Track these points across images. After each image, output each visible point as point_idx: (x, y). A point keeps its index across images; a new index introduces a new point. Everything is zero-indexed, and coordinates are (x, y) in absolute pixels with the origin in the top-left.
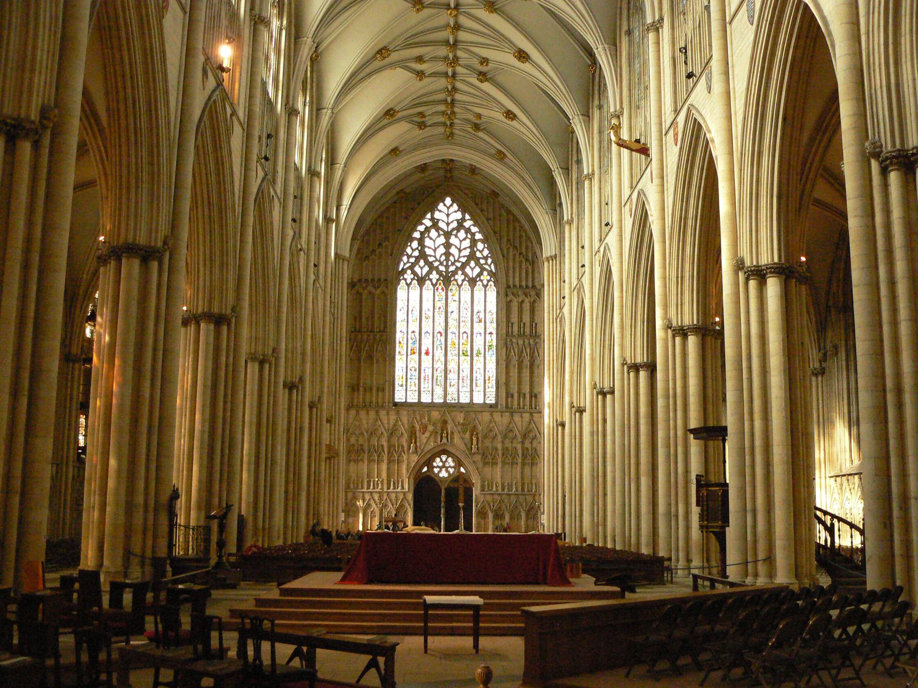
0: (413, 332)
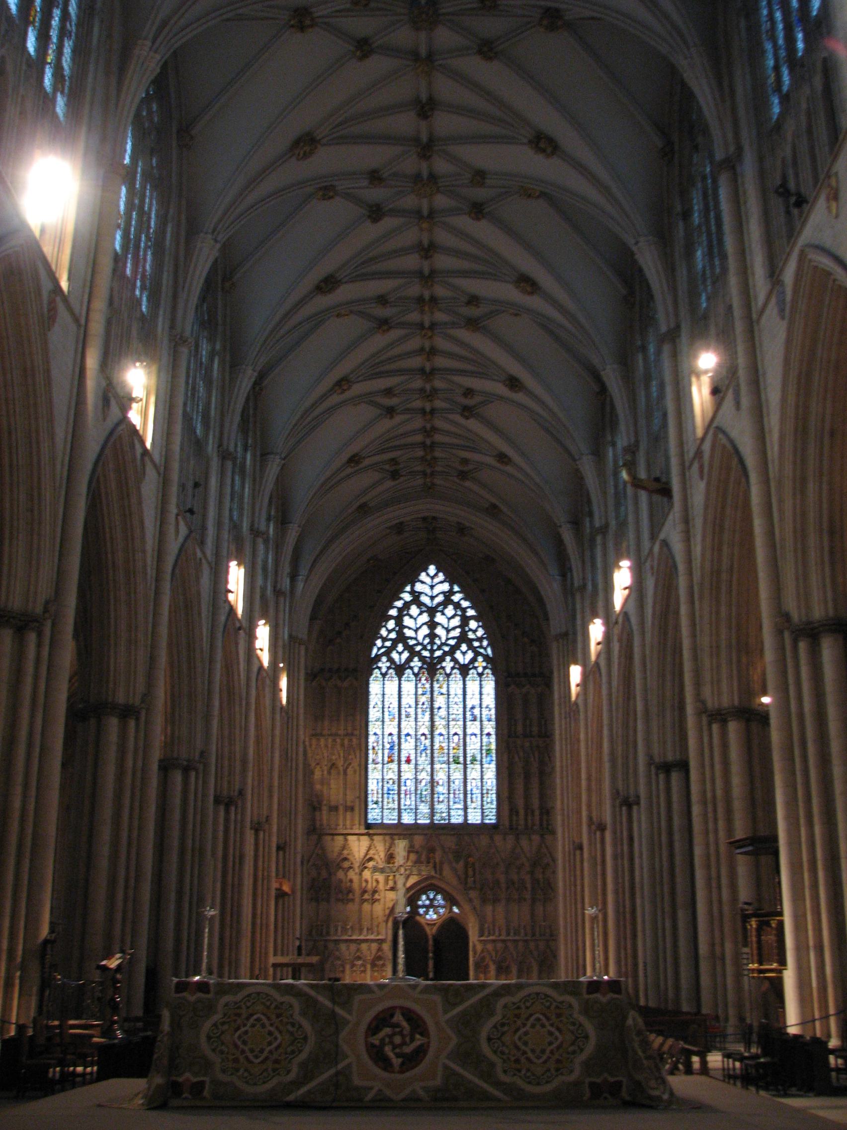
0: (390, 734)
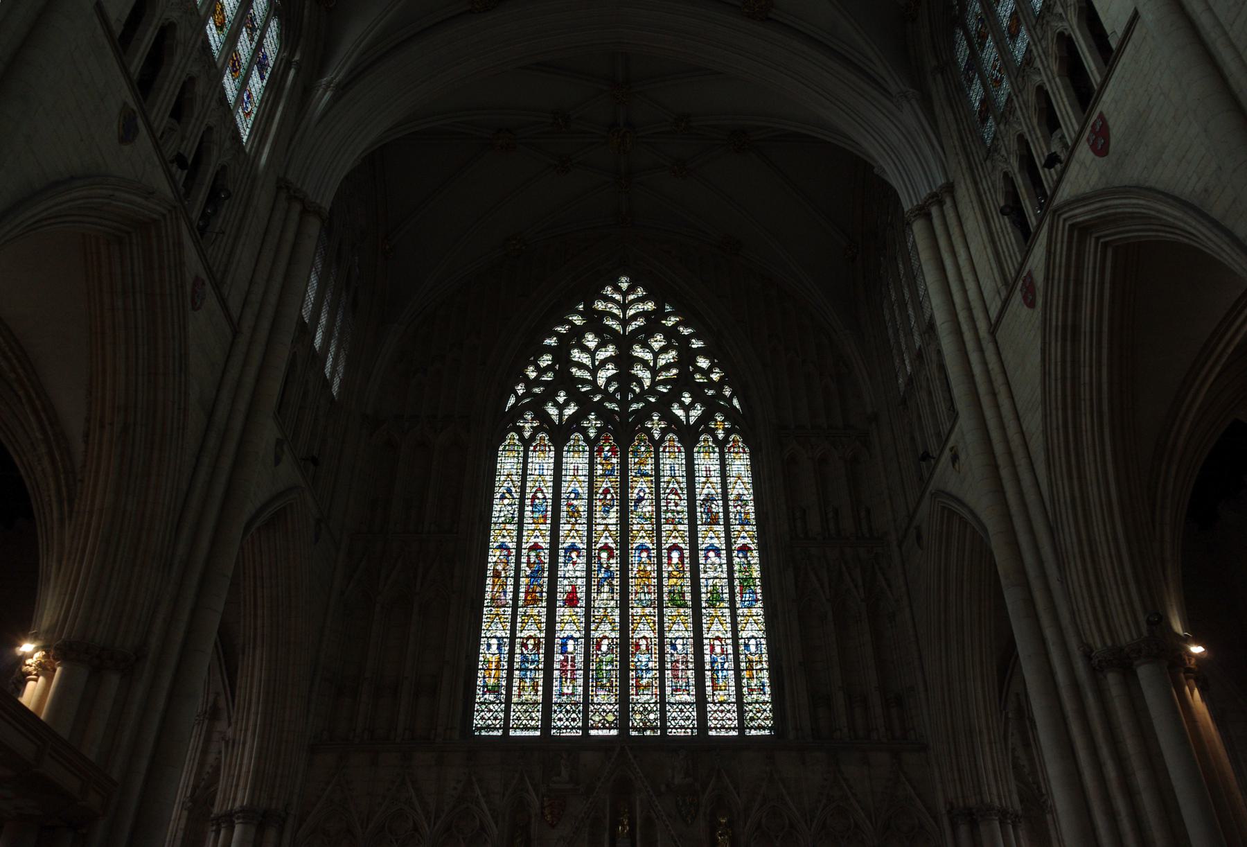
0: (535, 547)
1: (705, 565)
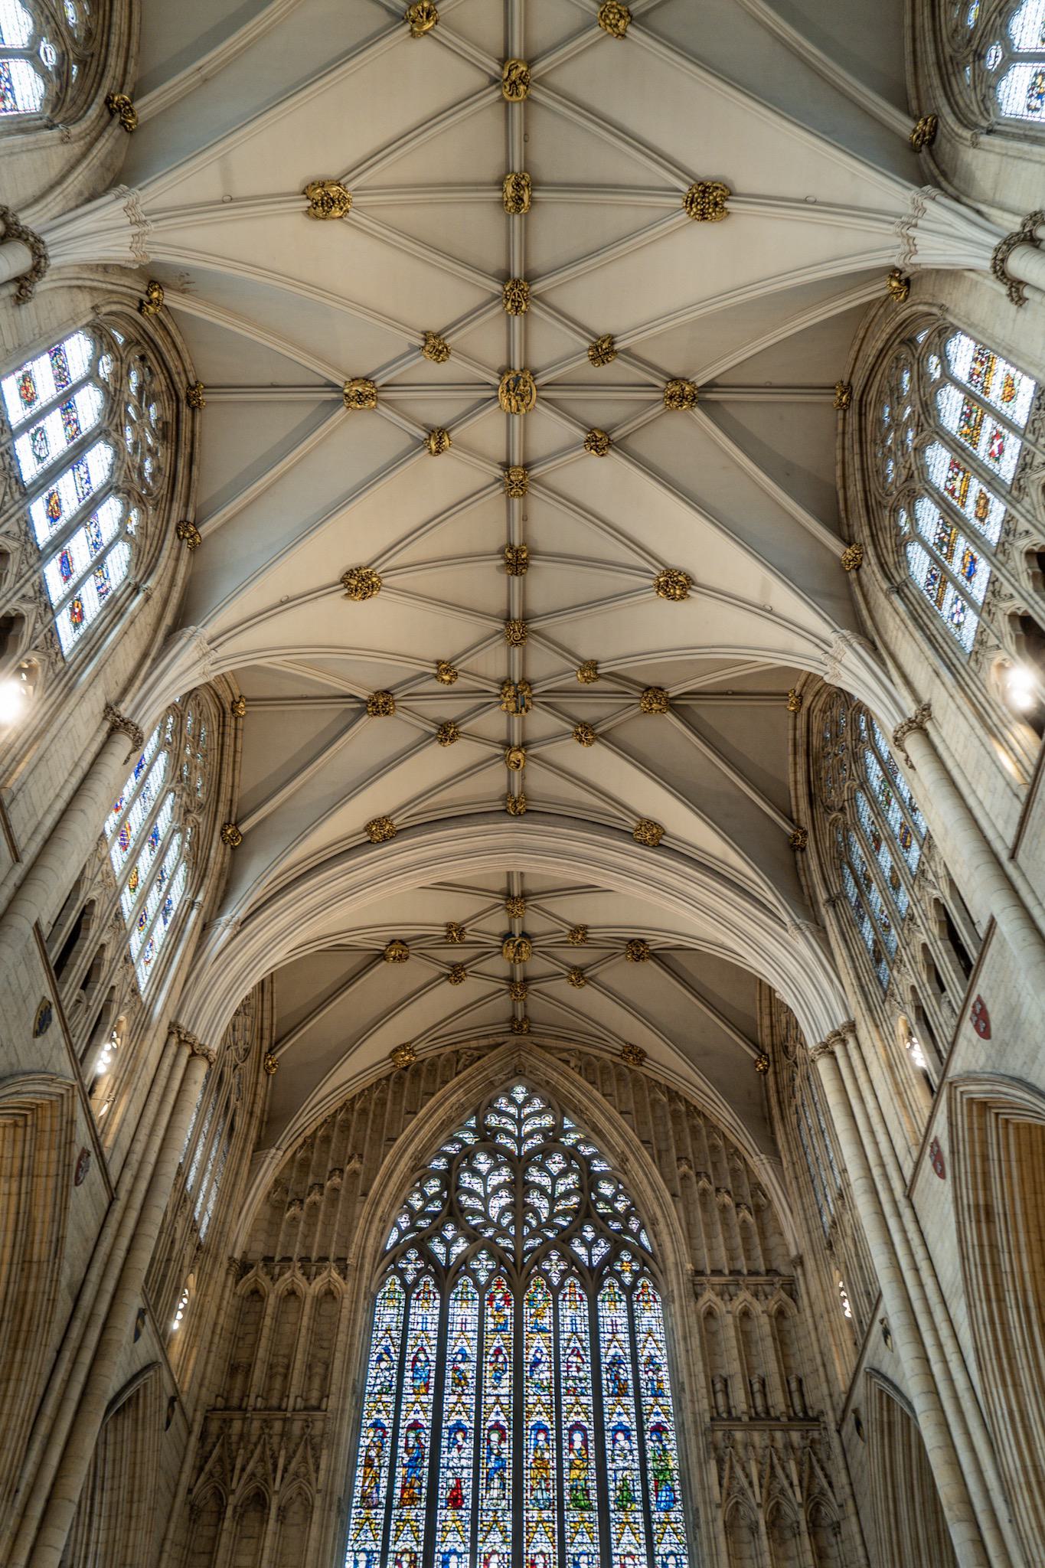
0: (415, 1426)
1: (612, 1451)
